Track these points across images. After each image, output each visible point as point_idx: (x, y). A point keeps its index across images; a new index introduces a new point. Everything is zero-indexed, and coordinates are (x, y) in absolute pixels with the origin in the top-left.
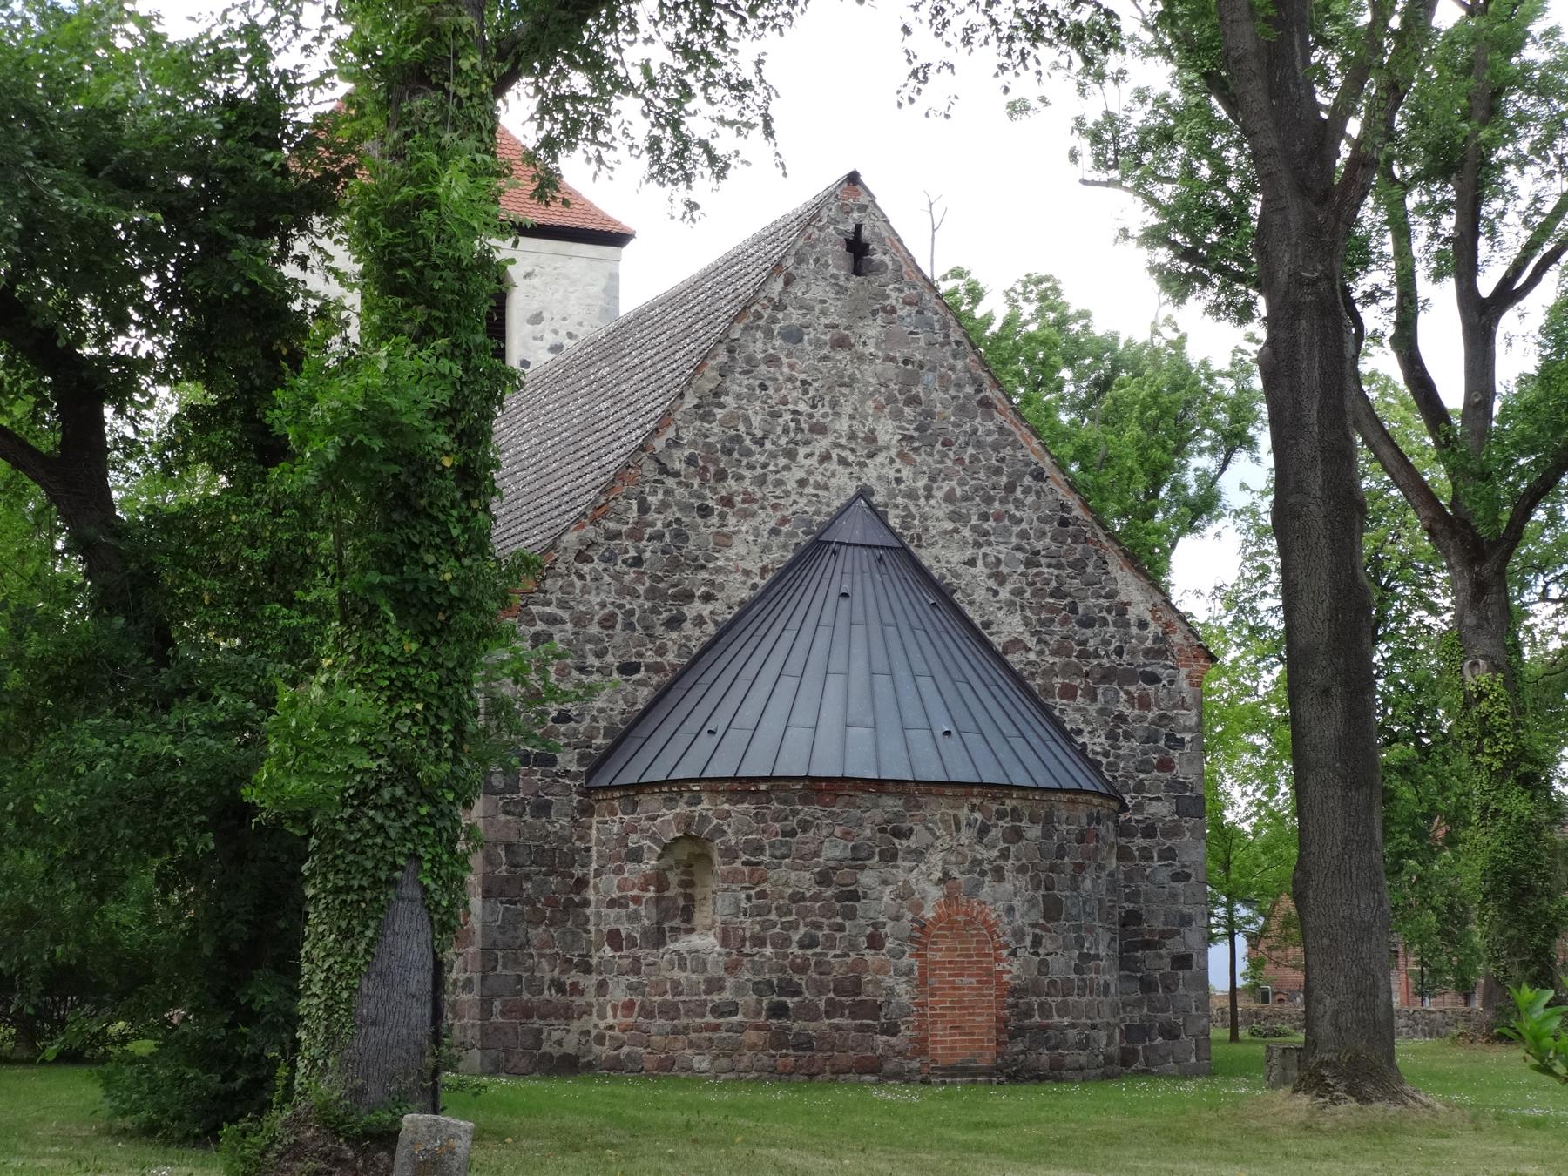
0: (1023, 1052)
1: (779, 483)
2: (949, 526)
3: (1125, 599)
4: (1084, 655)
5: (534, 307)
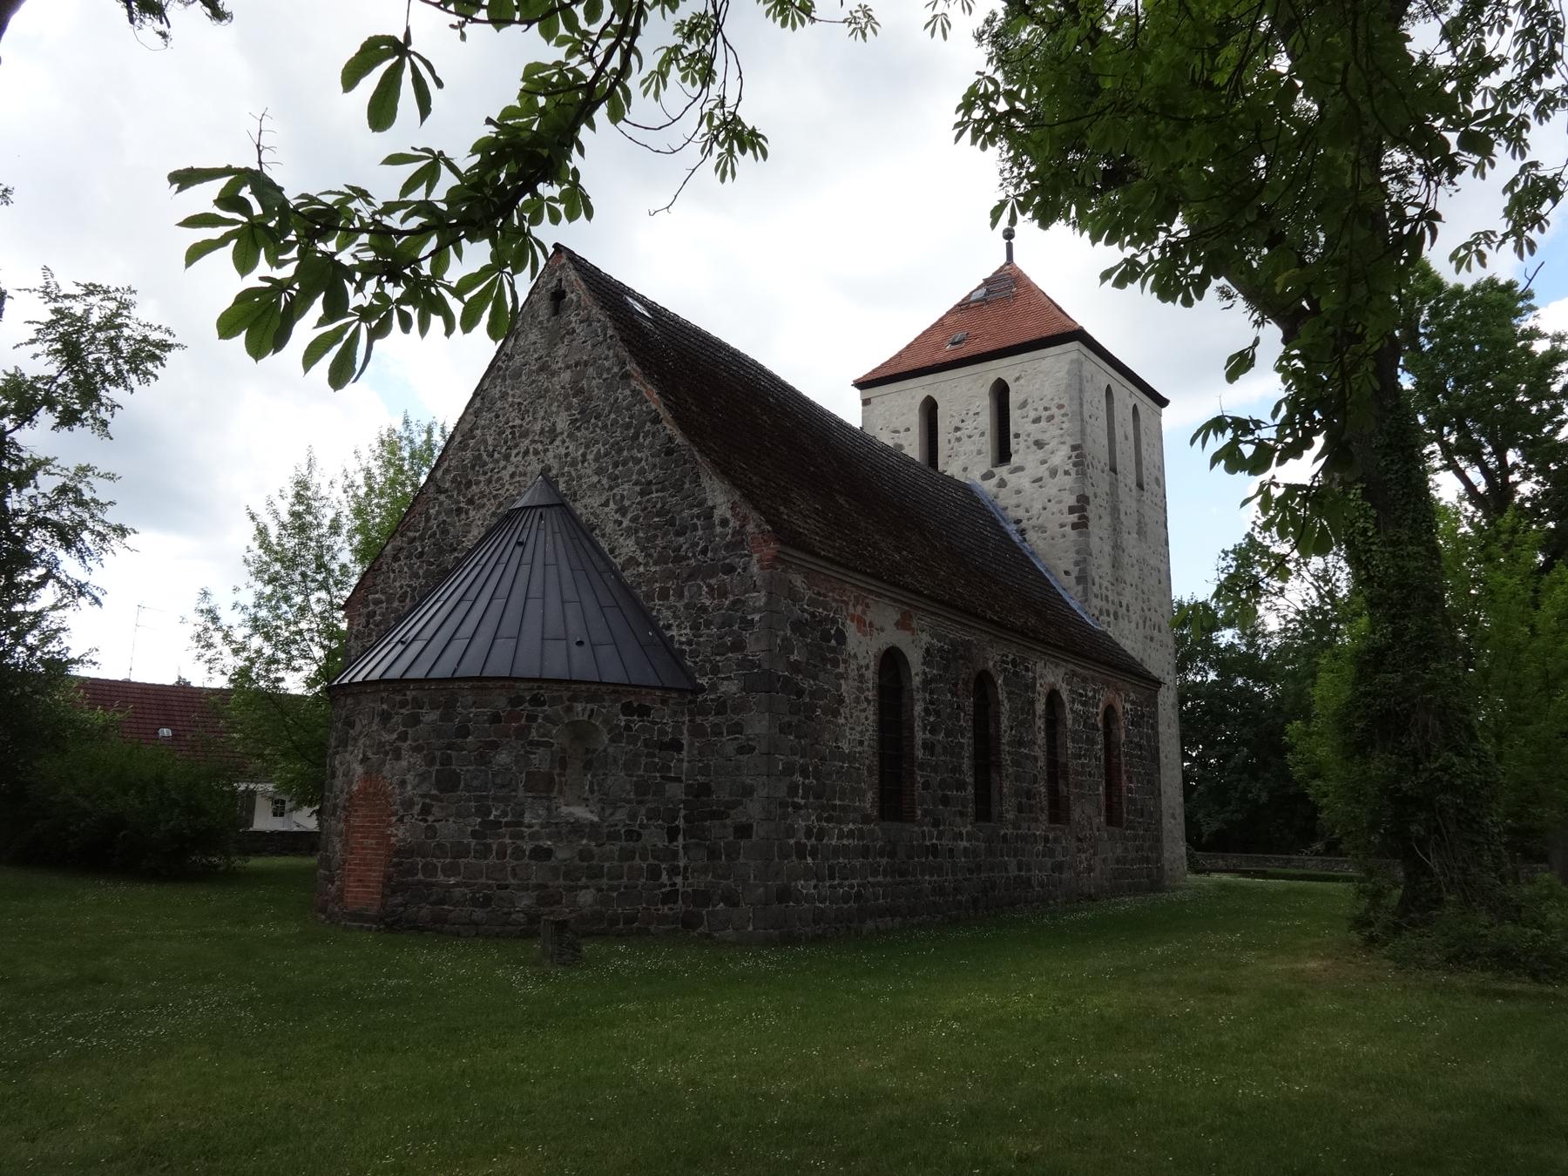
0: (405, 905)
1: (500, 479)
2: (595, 479)
3: (710, 503)
4: (678, 559)
5: (1022, 397)
